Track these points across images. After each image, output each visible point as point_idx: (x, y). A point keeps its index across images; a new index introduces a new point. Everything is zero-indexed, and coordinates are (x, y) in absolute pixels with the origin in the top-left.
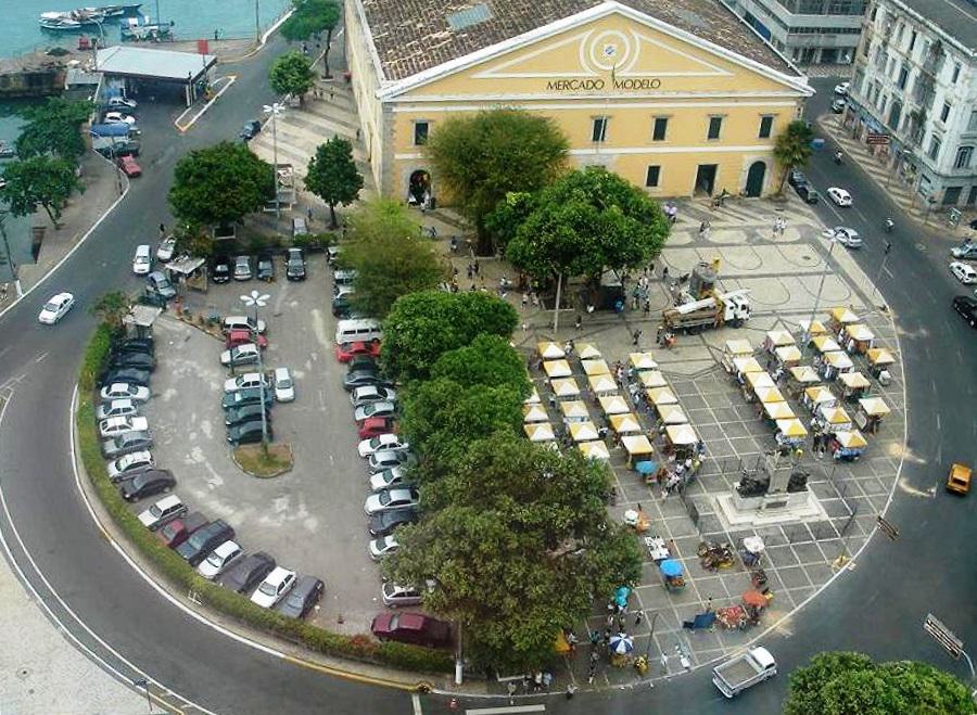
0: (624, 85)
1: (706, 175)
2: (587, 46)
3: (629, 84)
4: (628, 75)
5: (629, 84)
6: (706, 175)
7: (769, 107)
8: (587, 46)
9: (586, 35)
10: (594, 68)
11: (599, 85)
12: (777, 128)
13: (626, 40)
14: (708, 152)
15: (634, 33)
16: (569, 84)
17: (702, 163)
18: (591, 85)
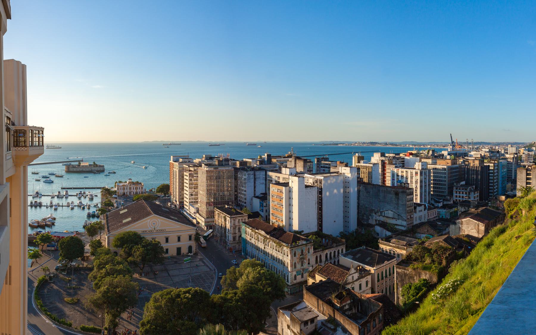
0: (158, 231)
1: (179, 249)
2: (149, 223)
3: (159, 231)
5: (159, 231)
6: (179, 249)
7: (190, 233)
8: (149, 223)
9: (149, 221)
10: (151, 228)
11: (152, 231)
12: (193, 237)
13: (157, 221)
14: (179, 244)
15: (159, 220)
17: (178, 247)
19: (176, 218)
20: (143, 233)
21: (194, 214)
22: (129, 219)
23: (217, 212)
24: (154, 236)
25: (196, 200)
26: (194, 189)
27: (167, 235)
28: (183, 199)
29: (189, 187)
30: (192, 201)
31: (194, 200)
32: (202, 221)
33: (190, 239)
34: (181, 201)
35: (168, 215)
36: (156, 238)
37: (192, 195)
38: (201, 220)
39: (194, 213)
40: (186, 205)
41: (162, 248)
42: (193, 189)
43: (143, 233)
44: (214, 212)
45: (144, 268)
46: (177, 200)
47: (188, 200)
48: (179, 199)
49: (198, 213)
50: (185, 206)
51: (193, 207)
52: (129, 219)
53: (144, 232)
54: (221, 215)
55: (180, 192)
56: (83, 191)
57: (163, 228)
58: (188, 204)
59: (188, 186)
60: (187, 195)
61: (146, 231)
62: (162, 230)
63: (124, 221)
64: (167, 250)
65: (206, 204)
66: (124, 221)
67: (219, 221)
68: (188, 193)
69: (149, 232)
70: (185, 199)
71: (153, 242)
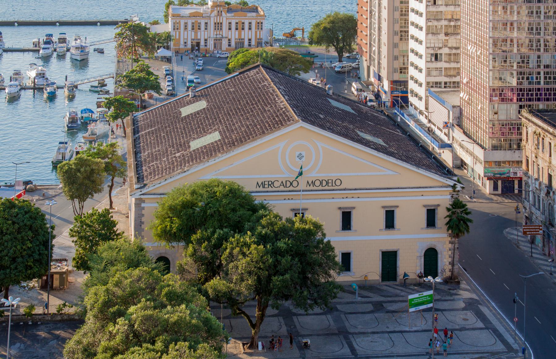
0: (313, 183)
3: (317, 183)
4: (318, 175)
5: (317, 183)
7: (432, 199)
12: (441, 215)
16: (273, 183)
18: (288, 184)
19: (380, 141)
20: (261, 189)
21: (446, 131)
22: (214, 137)
23: (531, 129)
24: (299, 203)
25: (450, 76)
26: (447, 34)
27: (347, 203)
28: (403, 70)
29: (428, 28)
30: (438, 79)
31: (446, 76)
32: (476, 158)
33: (431, 222)
34: (397, 77)
35: (351, 126)
36: (306, 209)
37: (436, 57)
38: (471, 154)
39: (446, 125)
40: (416, 95)
41: (329, 247)
42: (442, 37)
43: (261, 189)
44: (518, 128)
45: (266, 319)
46: (384, 74)
47: (421, 77)
48: (392, 70)
49: (460, 125)
50: (412, 99)
51: (442, 102)
52: (214, 137)
53: (263, 184)
54: (547, 140)
55: (393, 46)
56: (56, 33)
57: (333, 175)
58: (421, 91)
59: (422, 21)
60: (421, 57)
61: (271, 184)
62: (327, 183)
63: (196, 144)
64: (346, 257)
65: (491, 96)
66: (196, 144)
67: (540, 162)
68: (421, 49)
69: (282, 188)
70: (412, 71)
71: (297, 225)
